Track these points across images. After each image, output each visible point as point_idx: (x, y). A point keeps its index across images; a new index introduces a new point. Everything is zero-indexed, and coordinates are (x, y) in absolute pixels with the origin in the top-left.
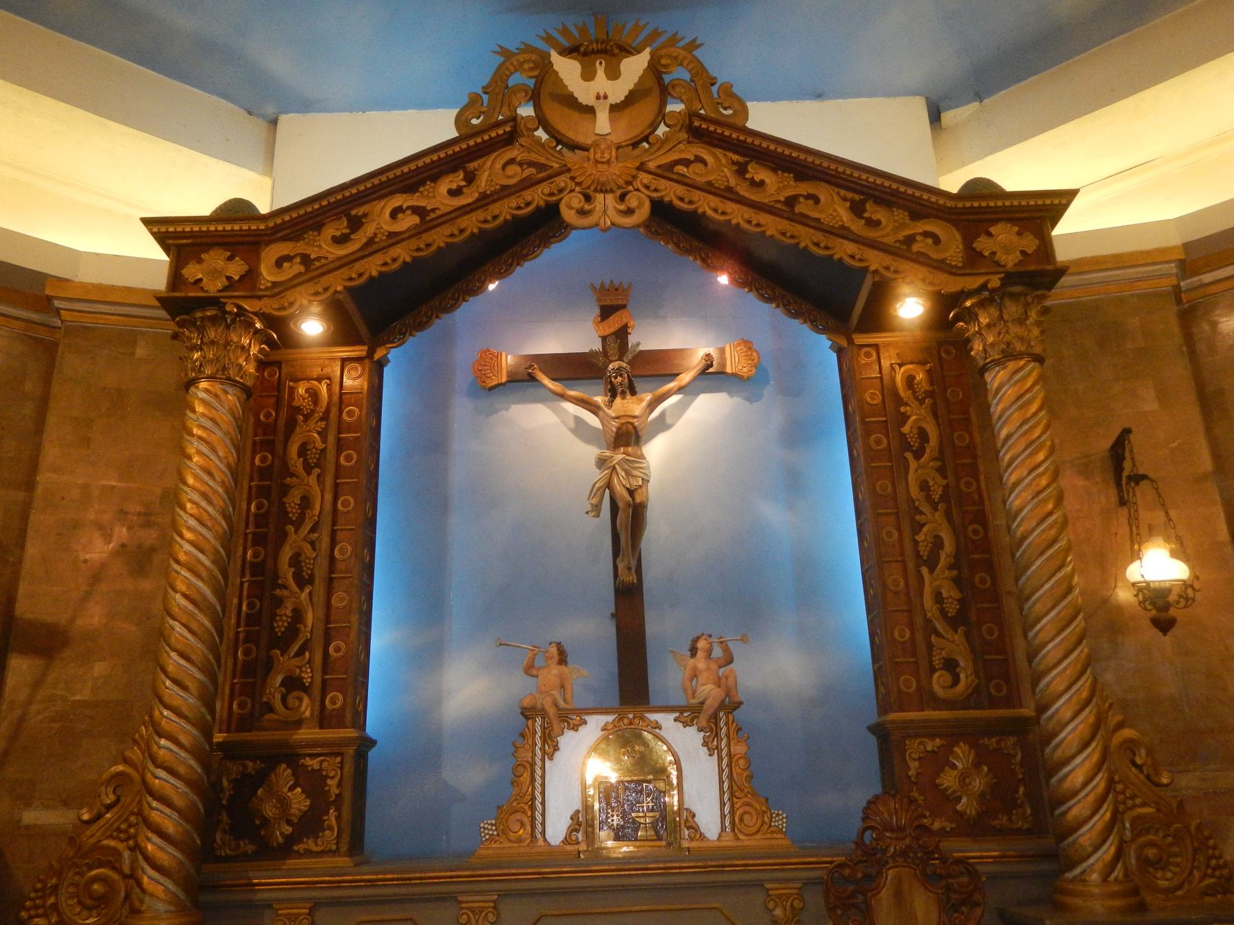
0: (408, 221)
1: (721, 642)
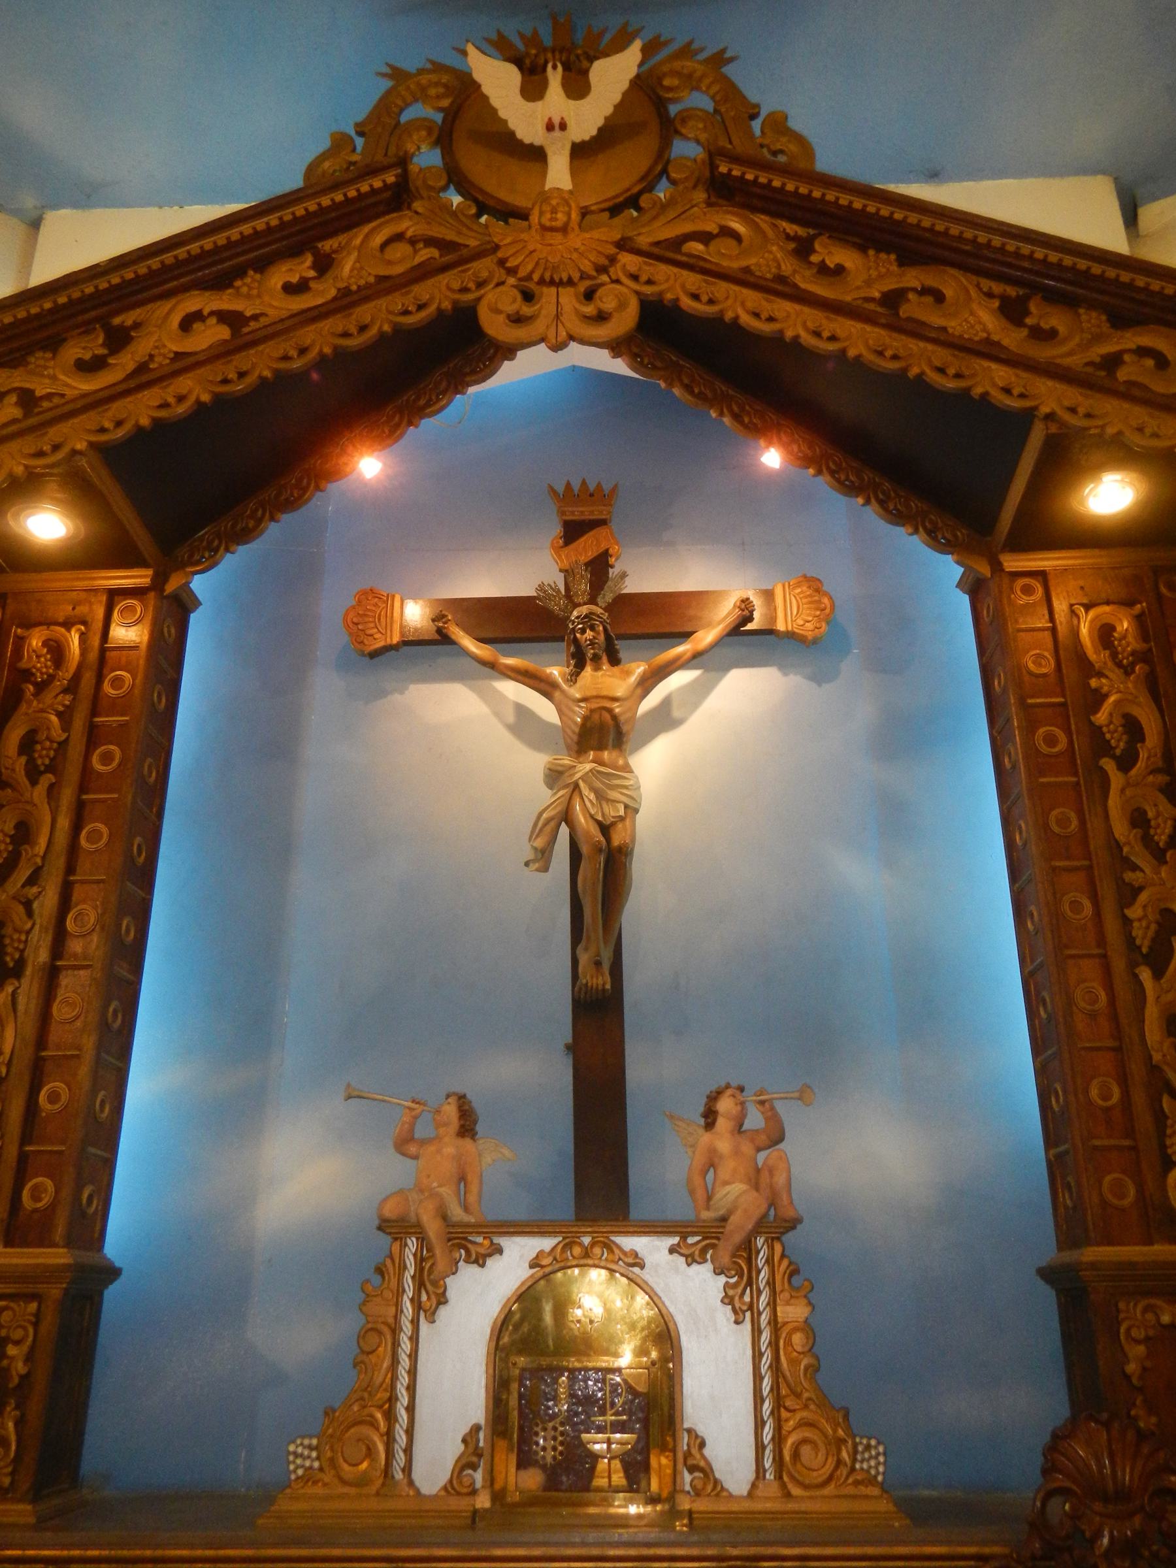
0: (211, 334)
1: (762, 1103)
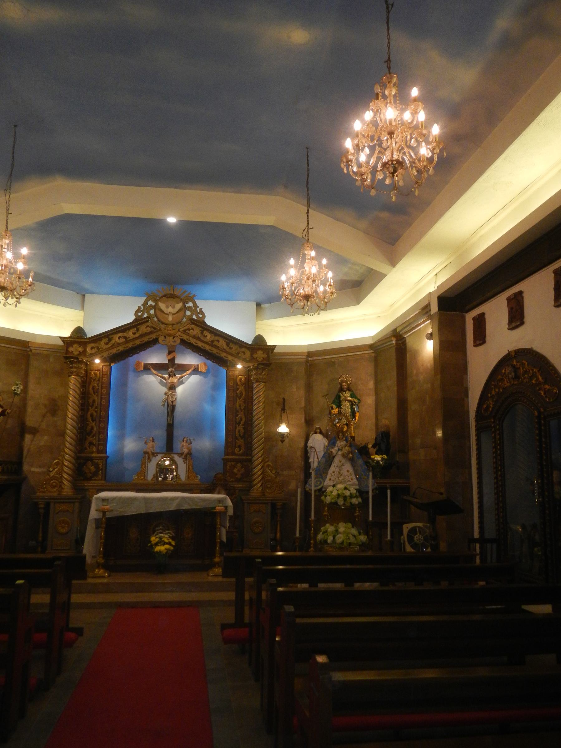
0: (122, 340)
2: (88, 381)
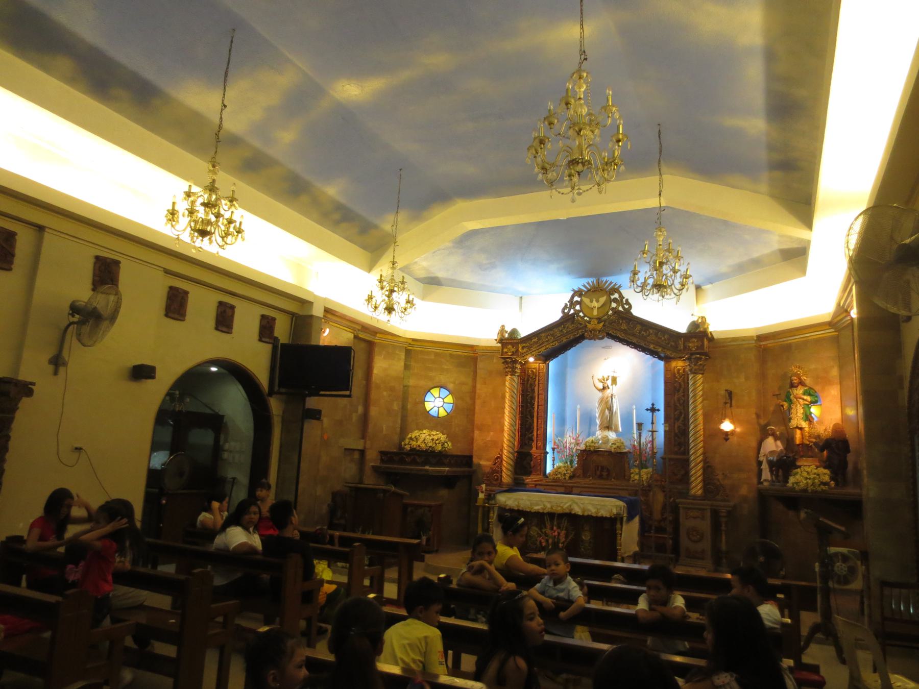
2: (526, 379)
